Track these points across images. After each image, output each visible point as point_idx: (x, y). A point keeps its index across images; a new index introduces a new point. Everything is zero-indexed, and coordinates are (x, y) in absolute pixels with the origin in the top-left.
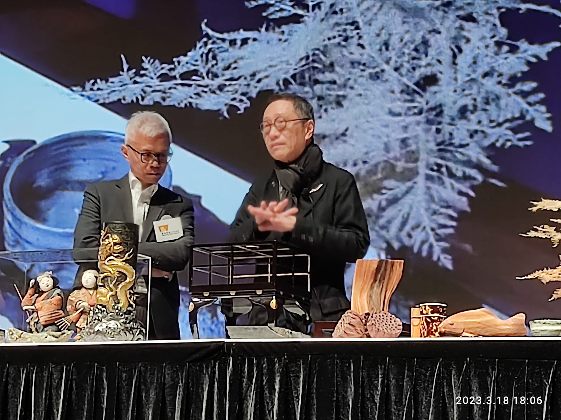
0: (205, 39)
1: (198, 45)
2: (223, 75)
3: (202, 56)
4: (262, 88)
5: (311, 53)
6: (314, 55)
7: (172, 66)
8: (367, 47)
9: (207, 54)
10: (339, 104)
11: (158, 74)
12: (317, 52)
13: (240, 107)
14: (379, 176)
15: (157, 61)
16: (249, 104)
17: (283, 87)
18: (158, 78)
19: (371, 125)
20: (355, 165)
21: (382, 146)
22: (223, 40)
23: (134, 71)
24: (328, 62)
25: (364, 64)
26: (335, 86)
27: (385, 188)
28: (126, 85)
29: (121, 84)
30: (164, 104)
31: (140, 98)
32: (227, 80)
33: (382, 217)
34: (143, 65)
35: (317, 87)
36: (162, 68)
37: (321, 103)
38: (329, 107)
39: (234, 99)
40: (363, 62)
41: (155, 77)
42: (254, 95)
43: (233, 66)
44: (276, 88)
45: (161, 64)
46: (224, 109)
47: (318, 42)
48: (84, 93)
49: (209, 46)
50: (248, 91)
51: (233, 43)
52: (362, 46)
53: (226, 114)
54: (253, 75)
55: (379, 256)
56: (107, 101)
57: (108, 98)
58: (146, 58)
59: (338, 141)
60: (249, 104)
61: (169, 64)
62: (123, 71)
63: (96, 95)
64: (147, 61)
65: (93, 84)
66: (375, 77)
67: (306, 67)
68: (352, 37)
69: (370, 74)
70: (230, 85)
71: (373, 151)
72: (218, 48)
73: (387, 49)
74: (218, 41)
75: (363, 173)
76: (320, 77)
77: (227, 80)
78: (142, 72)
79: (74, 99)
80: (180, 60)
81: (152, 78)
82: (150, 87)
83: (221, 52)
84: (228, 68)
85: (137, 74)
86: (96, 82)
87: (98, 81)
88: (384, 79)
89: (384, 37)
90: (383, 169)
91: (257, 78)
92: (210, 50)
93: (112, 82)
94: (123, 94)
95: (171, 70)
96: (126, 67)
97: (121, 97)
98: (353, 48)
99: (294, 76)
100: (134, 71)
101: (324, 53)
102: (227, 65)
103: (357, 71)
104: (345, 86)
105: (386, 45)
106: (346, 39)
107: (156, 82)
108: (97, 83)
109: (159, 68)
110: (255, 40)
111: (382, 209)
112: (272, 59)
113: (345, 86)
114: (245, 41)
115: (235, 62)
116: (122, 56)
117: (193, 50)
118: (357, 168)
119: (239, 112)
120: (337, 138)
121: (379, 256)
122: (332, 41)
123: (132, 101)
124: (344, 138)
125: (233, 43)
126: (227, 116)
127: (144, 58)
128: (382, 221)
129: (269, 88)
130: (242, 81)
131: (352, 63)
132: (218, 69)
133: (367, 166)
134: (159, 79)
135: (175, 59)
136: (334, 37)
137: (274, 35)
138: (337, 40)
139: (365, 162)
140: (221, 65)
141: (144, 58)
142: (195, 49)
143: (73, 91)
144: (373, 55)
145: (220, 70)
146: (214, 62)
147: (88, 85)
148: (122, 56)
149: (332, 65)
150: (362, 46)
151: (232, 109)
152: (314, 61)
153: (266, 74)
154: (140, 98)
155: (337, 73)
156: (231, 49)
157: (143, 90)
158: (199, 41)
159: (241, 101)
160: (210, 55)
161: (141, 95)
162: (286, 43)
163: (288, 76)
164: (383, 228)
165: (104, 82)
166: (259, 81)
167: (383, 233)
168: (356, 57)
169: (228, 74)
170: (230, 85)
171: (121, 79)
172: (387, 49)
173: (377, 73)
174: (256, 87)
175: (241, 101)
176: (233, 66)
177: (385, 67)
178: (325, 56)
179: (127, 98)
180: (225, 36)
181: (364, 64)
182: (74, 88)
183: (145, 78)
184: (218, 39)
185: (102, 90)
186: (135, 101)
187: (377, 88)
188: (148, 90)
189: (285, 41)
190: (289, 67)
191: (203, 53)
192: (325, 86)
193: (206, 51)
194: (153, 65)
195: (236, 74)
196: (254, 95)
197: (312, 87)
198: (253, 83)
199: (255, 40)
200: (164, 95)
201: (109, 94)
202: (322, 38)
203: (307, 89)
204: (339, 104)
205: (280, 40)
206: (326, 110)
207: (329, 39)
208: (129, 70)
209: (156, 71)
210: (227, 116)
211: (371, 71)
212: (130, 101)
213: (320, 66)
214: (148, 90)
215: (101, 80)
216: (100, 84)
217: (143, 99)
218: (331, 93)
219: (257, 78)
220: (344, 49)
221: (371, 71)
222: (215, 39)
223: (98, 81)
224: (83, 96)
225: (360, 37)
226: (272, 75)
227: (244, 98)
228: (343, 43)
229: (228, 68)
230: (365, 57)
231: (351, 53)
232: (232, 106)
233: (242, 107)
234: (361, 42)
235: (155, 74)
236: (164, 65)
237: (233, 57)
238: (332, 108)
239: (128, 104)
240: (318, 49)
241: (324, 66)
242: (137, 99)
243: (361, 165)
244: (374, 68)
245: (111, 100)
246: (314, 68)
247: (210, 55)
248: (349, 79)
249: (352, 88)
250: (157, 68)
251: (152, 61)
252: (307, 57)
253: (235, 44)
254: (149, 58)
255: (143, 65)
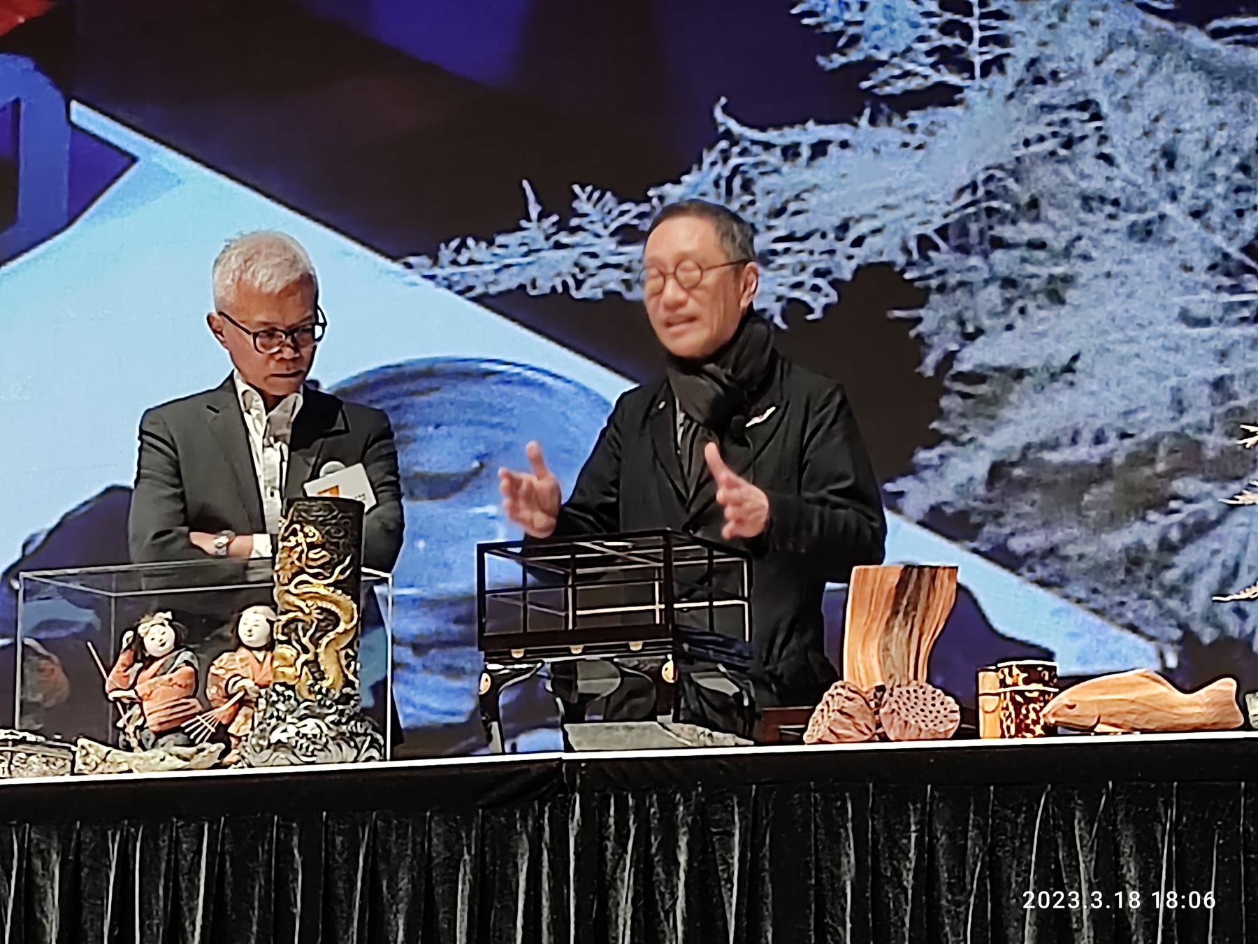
0: (723, 144)
1: (708, 158)
2: (770, 228)
3: (716, 184)
4: (867, 257)
5: (981, 177)
6: (990, 178)
7: (645, 207)
8: (1119, 159)
9: (729, 180)
10: (1056, 298)
11: (613, 226)
12: (999, 174)
13: (813, 305)
14: (1161, 467)
15: (608, 195)
16: (834, 297)
17: (915, 256)
18: (612, 235)
19: (1135, 348)
20: (1099, 439)
21: (1166, 398)
22: (768, 146)
23: (555, 218)
24: (1025, 199)
25: (1116, 203)
26: (1041, 255)
27: (1175, 497)
28: (538, 251)
29: (525, 249)
30: (628, 296)
31: (571, 282)
32: (778, 240)
33: (1168, 567)
34: (576, 204)
35: (998, 255)
36: (622, 213)
37: (1009, 294)
38: (1031, 306)
39: (798, 285)
40: (1113, 196)
41: (605, 233)
42: (847, 276)
43: (792, 207)
44: (901, 259)
45: (620, 202)
46: (776, 308)
47: (1003, 149)
48: (436, 271)
49: (734, 161)
50: (831, 265)
51: (790, 152)
52: (1107, 159)
53: (778, 320)
54: (844, 227)
55: (1162, 656)
56: (493, 290)
57: (495, 282)
58: (583, 188)
59: (1057, 385)
60: (834, 297)
61: (637, 203)
62: (529, 220)
63: (463, 274)
64: (584, 197)
65: (458, 250)
66: (1144, 233)
67: (971, 210)
68: (1083, 138)
69: (1133, 225)
70: (787, 250)
71: (1143, 408)
72: (756, 165)
73: (1171, 165)
74: (756, 149)
75: (1118, 460)
76: (1006, 232)
77: (778, 240)
78: (575, 222)
79: (414, 284)
80: (665, 194)
81: (598, 236)
82: (594, 255)
83: (763, 174)
84: (779, 213)
85: (562, 226)
86: (463, 245)
87: (470, 242)
88: (1165, 238)
89: (1162, 137)
90: (1172, 451)
91: (852, 235)
92: (736, 170)
93: (505, 246)
94: (532, 272)
95: (641, 216)
96: (534, 210)
97: (524, 279)
98: (1089, 164)
99: (942, 231)
100: (555, 218)
101: (1015, 174)
102: (778, 206)
103: (1098, 218)
104: (1067, 253)
105: (1170, 156)
106: (1069, 143)
107: (611, 245)
108: (468, 248)
109: (615, 213)
110: (844, 145)
111: (1167, 547)
112: (889, 191)
113: (1067, 253)
114: (820, 149)
115: (797, 197)
116: (525, 184)
117: (695, 167)
118: (1102, 449)
119: (810, 317)
120: (1053, 377)
121: (1162, 656)
122: (1035, 148)
123: (554, 289)
124: (1069, 376)
125: (790, 152)
126: (784, 326)
127: (577, 188)
128: (1171, 576)
129: (884, 258)
130: (815, 243)
131: (1087, 201)
132: (755, 213)
133: (1127, 442)
134: (617, 238)
135: (651, 193)
136: (1041, 139)
137: (891, 134)
138: (1050, 145)
139: (1124, 435)
140: (763, 204)
141: (577, 188)
142: (700, 169)
143: (409, 266)
144: (1140, 181)
145: (760, 218)
146: (748, 198)
147: (446, 254)
148: (525, 184)
149: (1034, 203)
150: (1107, 159)
151: (794, 309)
152: (990, 195)
153: (876, 224)
154: (571, 282)
155: (1052, 224)
156: (786, 168)
157: (576, 265)
158: (711, 147)
159: (816, 288)
160: (737, 182)
161: (574, 276)
162: (921, 152)
163: (929, 230)
164: (1172, 591)
165: (483, 245)
166: (858, 242)
167: (1173, 603)
168: (1095, 185)
169: (782, 226)
170: (787, 250)
171: (524, 237)
172: (1171, 165)
173: (1149, 222)
174: (850, 257)
175: (816, 288)
176: (792, 207)
177: (1168, 208)
178: (1017, 181)
179: (539, 283)
180: (771, 135)
181: (1116, 203)
182: (412, 260)
183: (578, 238)
184: (754, 142)
185: (480, 263)
186: (560, 289)
187: (1149, 259)
188: (592, 263)
189: (920, 147)
190: (930, 207)
191: (719, 177)
192: (1016, 253)
193: (726, 173)
194: (599, 206)
195: (800, 225)
196: (847, 276)
197: (985, 255)
198: (843, 247)
199: (844, 145)
200: (627, 276)
201: (497, 271)
202: (1009, 140)
203: (974, 261)
204: (1056, 298)
205: (905, 145)
206: (1022, 311)
207: (1027, 143)
208: (541, 216)
209: (607, 221)
210: (784, 326)
211: (1133, 217)
212: (548, 291)
213: (1008, 207)
214: (592, 263)
215: (477, 240)
216: (476, 250)
217: (579, 284)
218: (1030, 269)
219: (852, 235)
220: (1065, 169)
221: (1133, 217)
222: (747, 144)
223: (470, 242)
224: (432, 277)
225: (1103, 139)
226: (892, 227)
227: (820, 282)
228: (1063, 152)
229: (779, 213)
230: (1118, 184)
231: (1083, 176)
232: (792, 301)
233: (818, 304)
234: (1106, 149)
235: (606, 227)
236: (625, 207)
237: (794, 186)
238: (1039, 307)
239: (544, 296)
240: (1001, 167)
241: (1017, 206)
242: (565, 284)
243: (1113, 441)
244: (1141, 210)
245: (502, 287)
246: (990, 211)
247: (737, 182)
248: (1079, 238)
249: (1086, 258)
250: (610, 212)
251: (596, 195)
252: (973, 186)
253: (798, 155)
254: (589, 189)
255: (576, 204)
